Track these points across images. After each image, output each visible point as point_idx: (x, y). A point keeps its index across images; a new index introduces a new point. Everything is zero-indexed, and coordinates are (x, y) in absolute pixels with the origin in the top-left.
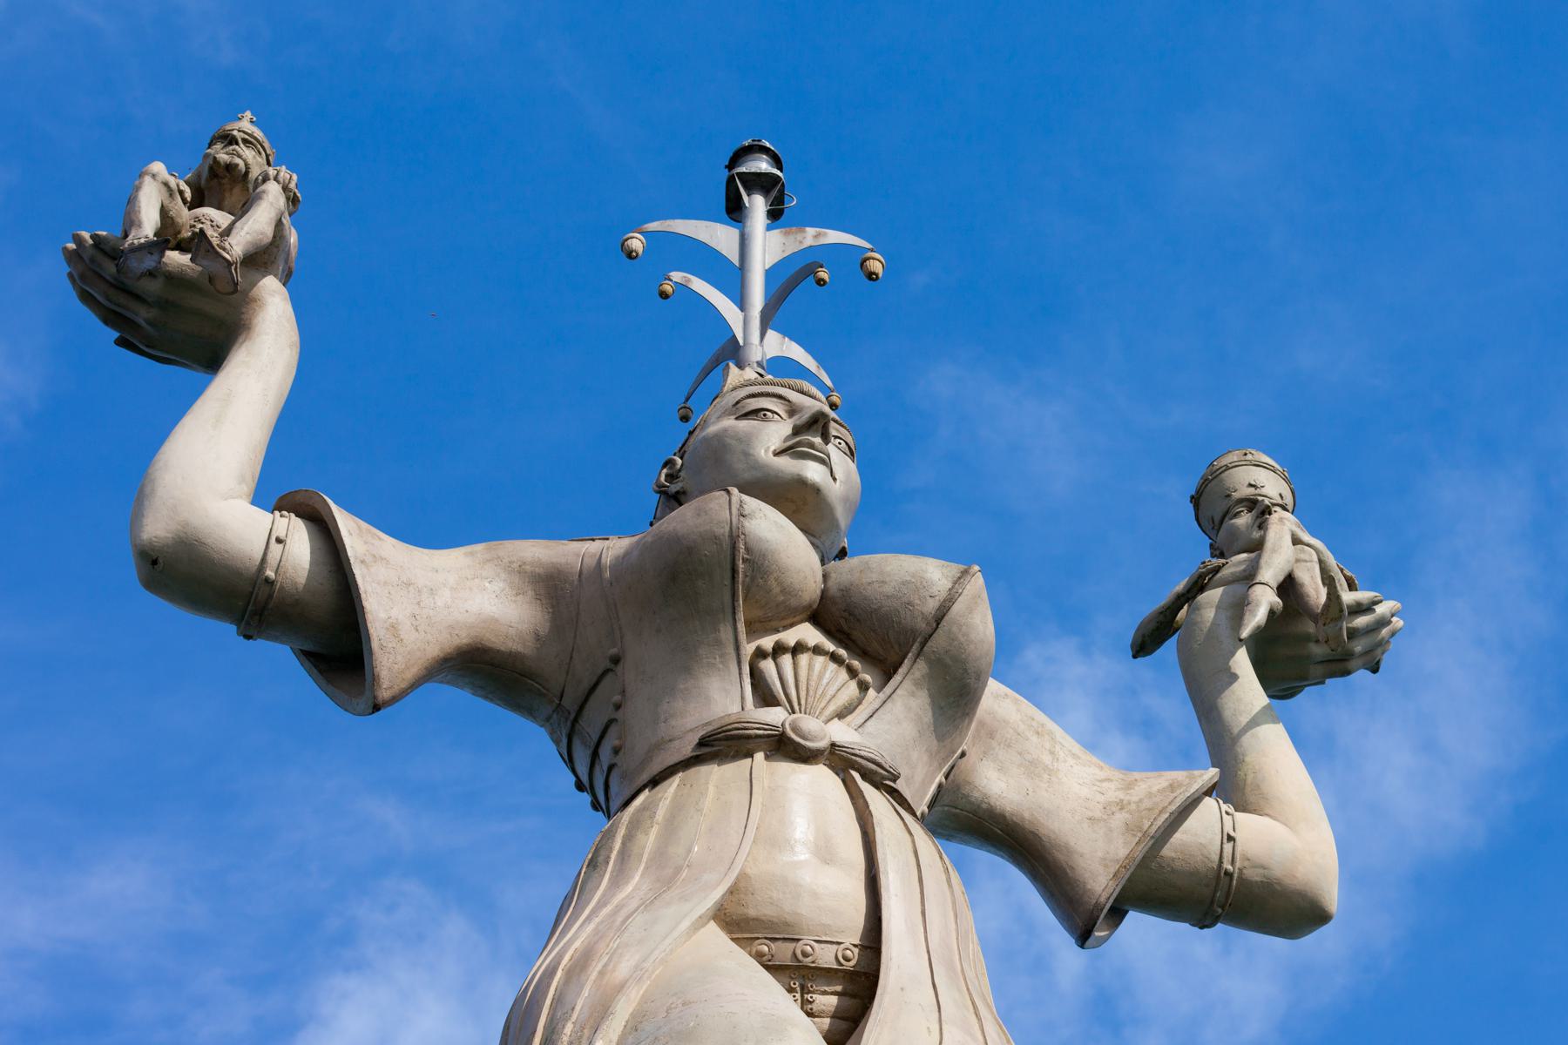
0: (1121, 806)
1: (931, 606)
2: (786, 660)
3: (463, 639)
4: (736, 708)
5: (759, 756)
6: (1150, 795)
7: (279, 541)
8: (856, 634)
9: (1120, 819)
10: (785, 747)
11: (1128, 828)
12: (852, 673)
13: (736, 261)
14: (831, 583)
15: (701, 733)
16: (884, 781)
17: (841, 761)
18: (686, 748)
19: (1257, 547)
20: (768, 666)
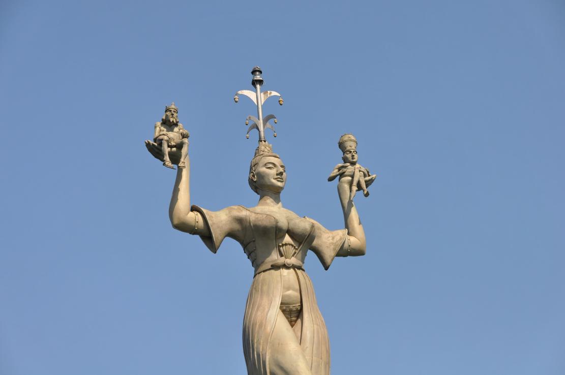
0: (332, 243)
1: (309, 233)
2: (284, 247)
3: (227, 233)
4: (277, 258)
5: (281, 269)
6: (337, 241)
7: (197, 222)
8: (294, 237)
9: (332, 247)
10: (285, 266)
11: (334, 249)
12: (295, 247)
13: (255, 101)
14: (290, 224)
15: (271, 264)
16: (300, 268)
17: (294, 267)
18: (270, 267)
19: (352, 176)
20: (281, 248)
